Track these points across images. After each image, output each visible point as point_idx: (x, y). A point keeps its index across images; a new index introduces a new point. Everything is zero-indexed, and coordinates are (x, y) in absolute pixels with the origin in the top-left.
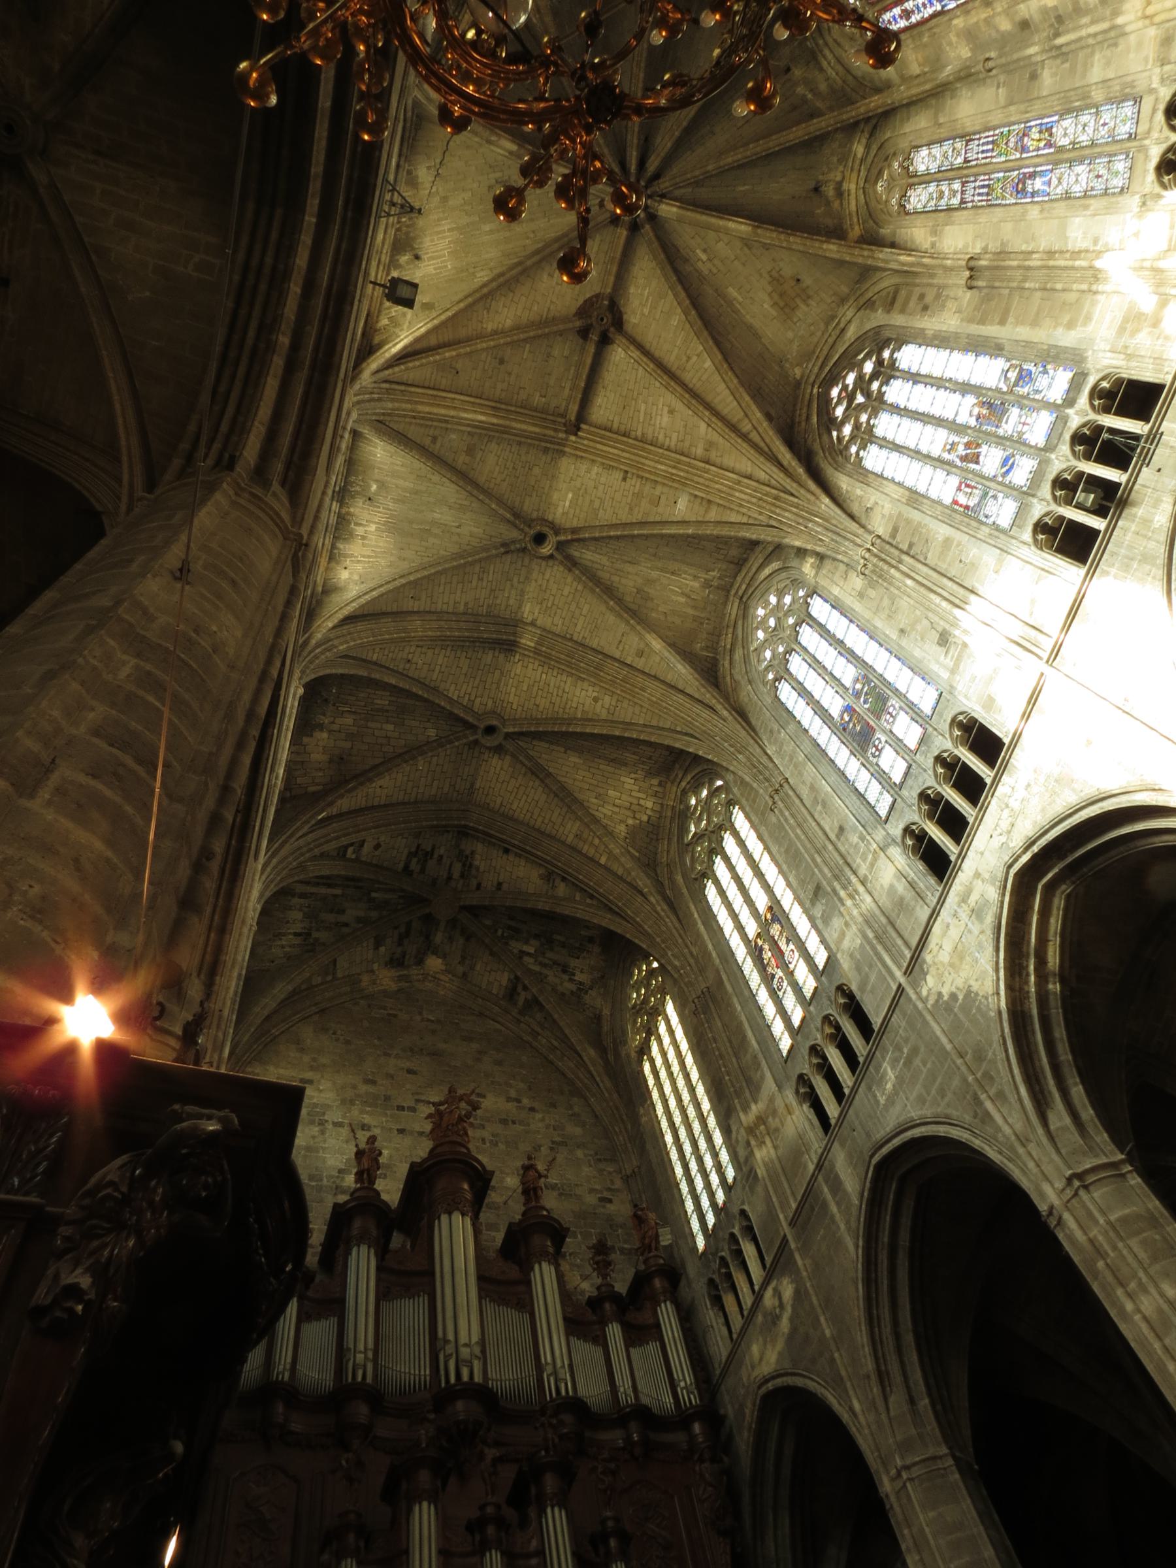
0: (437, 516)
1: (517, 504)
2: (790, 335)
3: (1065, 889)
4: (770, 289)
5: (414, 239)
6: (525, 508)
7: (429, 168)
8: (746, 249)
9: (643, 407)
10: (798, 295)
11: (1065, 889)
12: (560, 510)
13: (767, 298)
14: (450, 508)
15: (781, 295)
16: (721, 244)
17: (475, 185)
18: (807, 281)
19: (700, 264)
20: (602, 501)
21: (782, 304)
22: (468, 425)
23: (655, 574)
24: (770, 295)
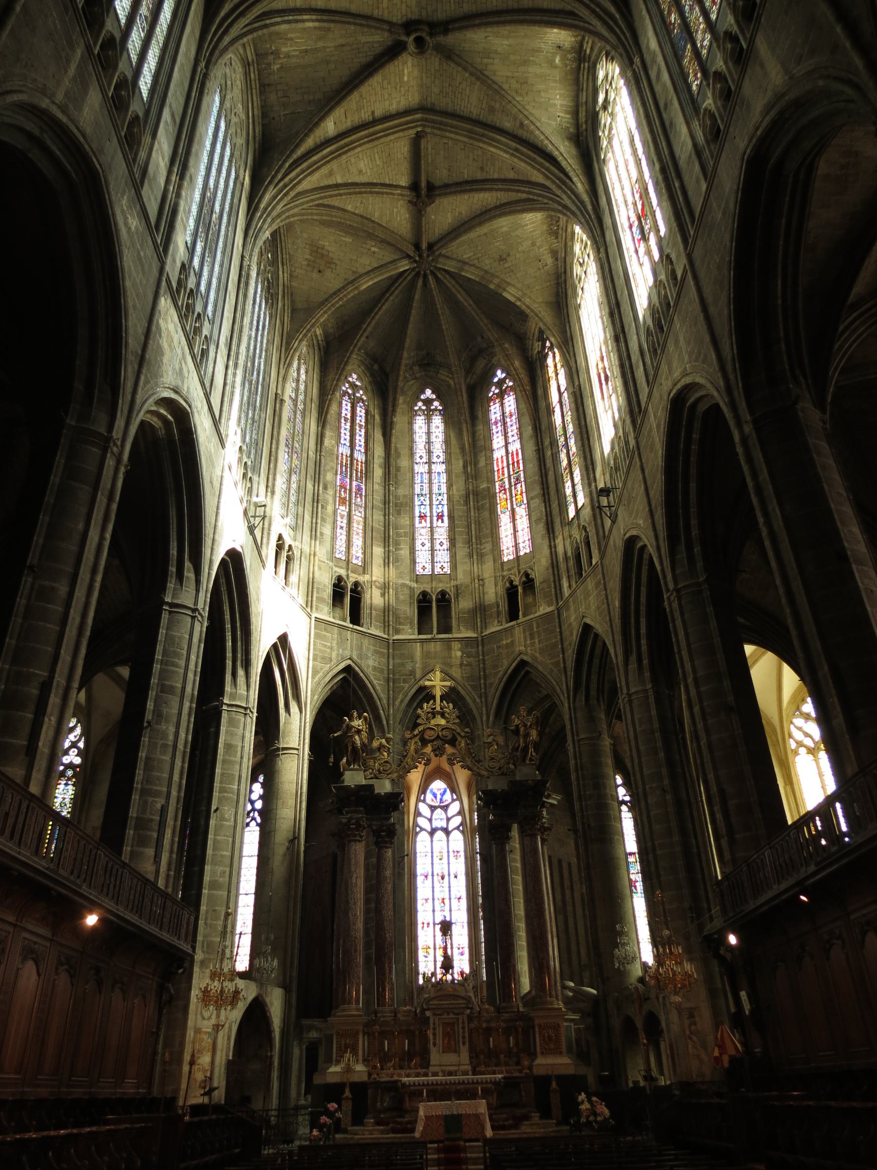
0: (506, 42)
1: (445, 64)
2: (305, 235)
3: (162, 433)
4: (331, 255)
5: (548, 217)
6: (437, 60)
7: (546, 265)
8: (354, 269)
9: (378, 162)
10: (314, 262)
11: (162, 433)
12: (410, 64)
13: (329, 248)
14: (496, 52)
15: (323, 255)
16: (368, 263)
17: (518, 256)
18: (315, 275)
19: (373, 244)
20: (383, 88)
21: (319, 250)
22: (498, 141)
23: (320, 44)
24: (329, 251)
